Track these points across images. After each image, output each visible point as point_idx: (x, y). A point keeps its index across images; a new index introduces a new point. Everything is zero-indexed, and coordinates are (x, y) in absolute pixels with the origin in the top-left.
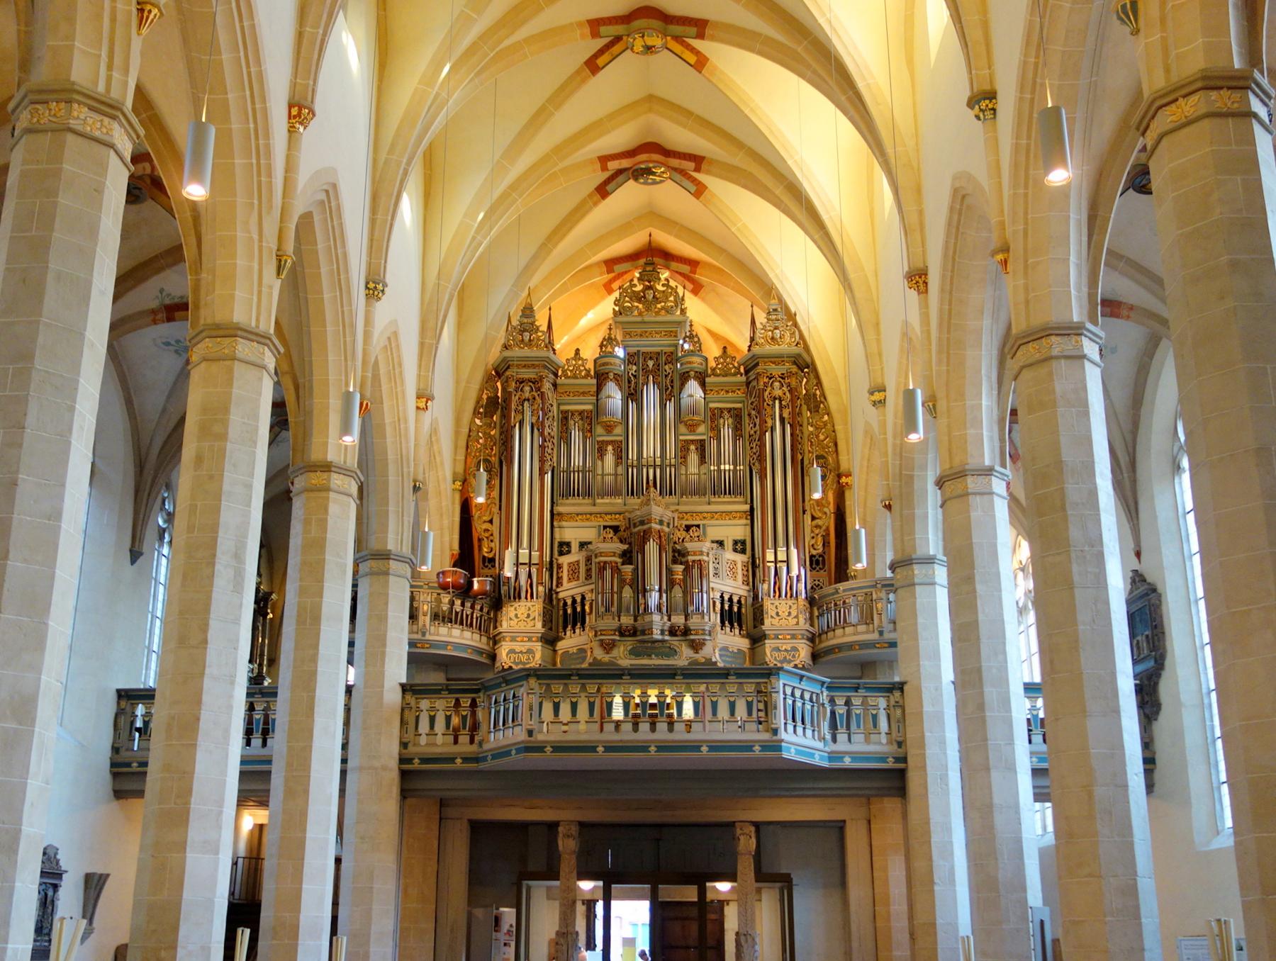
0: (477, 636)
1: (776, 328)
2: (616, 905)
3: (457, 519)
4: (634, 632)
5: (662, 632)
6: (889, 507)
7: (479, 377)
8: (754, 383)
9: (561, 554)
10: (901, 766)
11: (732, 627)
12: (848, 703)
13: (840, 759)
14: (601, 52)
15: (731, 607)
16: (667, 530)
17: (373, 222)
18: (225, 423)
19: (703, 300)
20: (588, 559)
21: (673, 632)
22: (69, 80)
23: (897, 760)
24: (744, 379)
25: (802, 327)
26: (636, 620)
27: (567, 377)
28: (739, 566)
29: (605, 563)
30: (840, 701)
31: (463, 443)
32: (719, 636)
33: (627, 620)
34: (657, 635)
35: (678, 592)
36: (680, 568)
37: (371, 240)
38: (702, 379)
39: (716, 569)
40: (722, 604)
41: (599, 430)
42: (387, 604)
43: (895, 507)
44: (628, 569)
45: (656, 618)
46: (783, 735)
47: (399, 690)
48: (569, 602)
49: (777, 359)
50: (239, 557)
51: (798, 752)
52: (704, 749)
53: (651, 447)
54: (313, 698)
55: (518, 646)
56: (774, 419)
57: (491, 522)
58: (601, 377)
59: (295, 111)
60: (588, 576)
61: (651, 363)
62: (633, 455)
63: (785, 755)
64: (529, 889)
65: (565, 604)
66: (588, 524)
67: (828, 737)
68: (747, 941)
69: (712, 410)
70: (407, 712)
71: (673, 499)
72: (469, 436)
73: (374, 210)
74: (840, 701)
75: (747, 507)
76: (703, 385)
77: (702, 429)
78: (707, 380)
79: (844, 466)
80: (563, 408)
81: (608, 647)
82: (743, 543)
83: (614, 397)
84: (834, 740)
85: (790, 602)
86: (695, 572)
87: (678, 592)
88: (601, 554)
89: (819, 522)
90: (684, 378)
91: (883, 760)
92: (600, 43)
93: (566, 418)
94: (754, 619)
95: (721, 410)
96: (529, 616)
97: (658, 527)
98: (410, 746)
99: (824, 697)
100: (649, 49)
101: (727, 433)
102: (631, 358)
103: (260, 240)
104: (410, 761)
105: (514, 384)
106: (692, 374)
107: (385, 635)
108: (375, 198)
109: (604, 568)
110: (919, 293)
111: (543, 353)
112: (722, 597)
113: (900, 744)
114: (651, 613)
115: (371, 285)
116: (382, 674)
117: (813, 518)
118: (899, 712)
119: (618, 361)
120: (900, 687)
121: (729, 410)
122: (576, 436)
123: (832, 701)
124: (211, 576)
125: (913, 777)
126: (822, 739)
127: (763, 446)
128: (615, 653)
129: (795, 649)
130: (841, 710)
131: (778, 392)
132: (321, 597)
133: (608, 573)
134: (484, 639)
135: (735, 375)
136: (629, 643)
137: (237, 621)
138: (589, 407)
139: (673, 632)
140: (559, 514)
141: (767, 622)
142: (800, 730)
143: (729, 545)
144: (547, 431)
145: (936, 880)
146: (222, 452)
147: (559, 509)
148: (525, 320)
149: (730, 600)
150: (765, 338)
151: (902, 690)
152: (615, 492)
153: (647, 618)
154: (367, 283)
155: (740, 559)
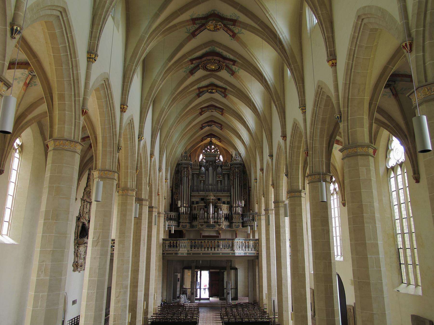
0: (175, 222)
1: (237, 158)
2: (202, 272)
3: (171, 196)
4: (207, 222)
5: (213, 223)
6: (257, 203)
7: (175, 166)
8: (232, 168)
9: (192, 204)
10: (258, 255)
11: (227, 220)
12: (248, 242)
13: (246, 254)
14: (196, 30)
15: (226, 216)
16: (214, 201)
17: (160, 156)
18: (141, 217)
19: (222, 143)
20: (198, 206)
21: (215, 222)
22: (127, 187)
23: (257, 254)
24: (230, 167)
25: (242, 157)
26: (207, 220)
27: (194, 166)
28: (228, 207)
29: (201, 208)
30: (247, 242)
31: (172, 180)
32: (224, 222)
33: (206, 220)
34: (212, 223)
35: (216, 214)
36: (216, 209)
37: (159, 160)
38: (221, 167)
39: (224, 209)
40: (225, 216)
41: (200, 177)
42: (160, 223)
43: (258, 203)
44: (206, 209)
45: (212, 220)
46: (236, 251)
47: (162, 240)
48: (194, 214)
49: (236, 164)
50: (144, 240)
51: (238, 254)
52: (221, 254)
53: (210, 181)
54: (151, 252)
55: (184, 224)
56: (236, 177)
57: (178, 197)
58: (201, 166)
59: (151, 156)
60: (198, 210)
61: (211, 163)
62: (207, 183)
63: (236, 255)
64: (184, 271)
65: (193, 215)
66: (198, 198)
67: (244, 250)
68: (228, 283)
69: (223, 173)
70: (164, 245)
71: (215, 193)
72: (173, 178)
73: (160, 154)
74: (247, 242)
75: (230, 195)
76: (221, 168)
77: (221, 178)
78: (223, 167)
79: (250, 186)
80: (193, 172)
81: (202, 225)
82: (229, 202)
83: (203, 168)
84: (245, 250)
85: (238, 215)
86: (219, 210)
87: (216, 214)
88: (201, 206)
89: (245, 198)
90: (218, 166)
91: (254, 254)
92: (197, 26)
93: (193, 175)
94: (231, 218)
95: (225, 173)
96: (186, 218)
97: (212, 201)
98: (164, 251)
99: (244, 242)
100: (212, 111)
101: (226, 178)
102: (207, 162)
103: (146, 182)
104: (164, 254)
105: (183, 168)
106: (219, 166)
107: (160, 229)
108: (160, 151)
109: (201, 209)
110: (262, 173)
111: (189, 162)
112: (225, 214)
113: (257, 251)
114: (211, 219)
115: (160, 170)
116: (159, 237)
117: (243, 197)
118: (257, 245)
119: (204, 163)
120: (258, 240)
121: (227, 173)
122: (195, 178)
123: (245, 243)
124: (140, 244)
125: (260, 257)
126: (243, 250)
127: (234, 182)
128: (203, 227)
129: (239, 225)
130: (247, 244)
131: (237, 171)
132: (152, 232)
133: (202, 210)
134: (177, 223)
135: (228, 166)
136: (206, 224)
137: (144, 252)
138: (198, 172)
139: (215, 222)
140: (192, 196)
141: (233, 220)
142: (239, 249)
143: (226, 203)
144: (190, 178)
145: (263, 277)
146: (141, 222)
147: (191, 195)
148: (185, 155)
149: (226, 214)
150: (234, 160)
151: (258, 240)
152: (204, 191)
153: (210, 220)
154: (159, 169)
155: (228, 206)
